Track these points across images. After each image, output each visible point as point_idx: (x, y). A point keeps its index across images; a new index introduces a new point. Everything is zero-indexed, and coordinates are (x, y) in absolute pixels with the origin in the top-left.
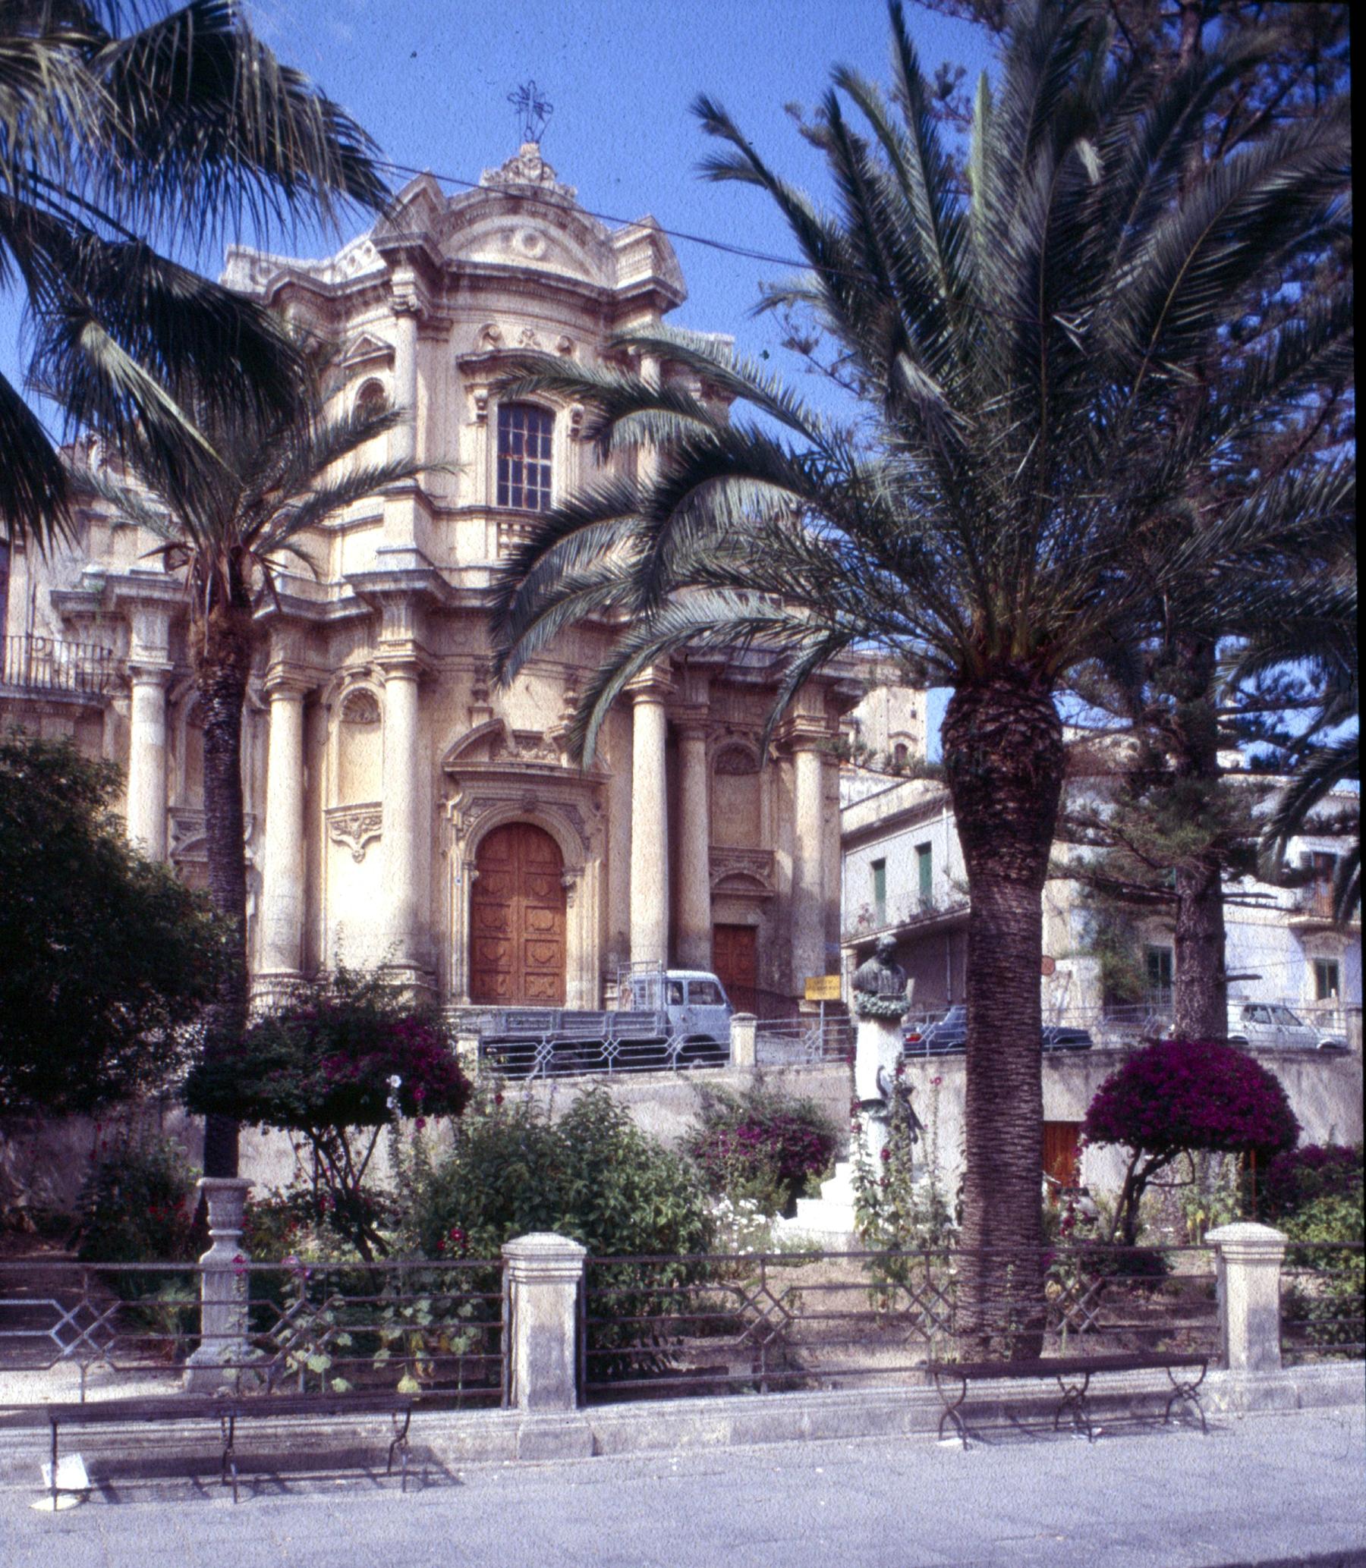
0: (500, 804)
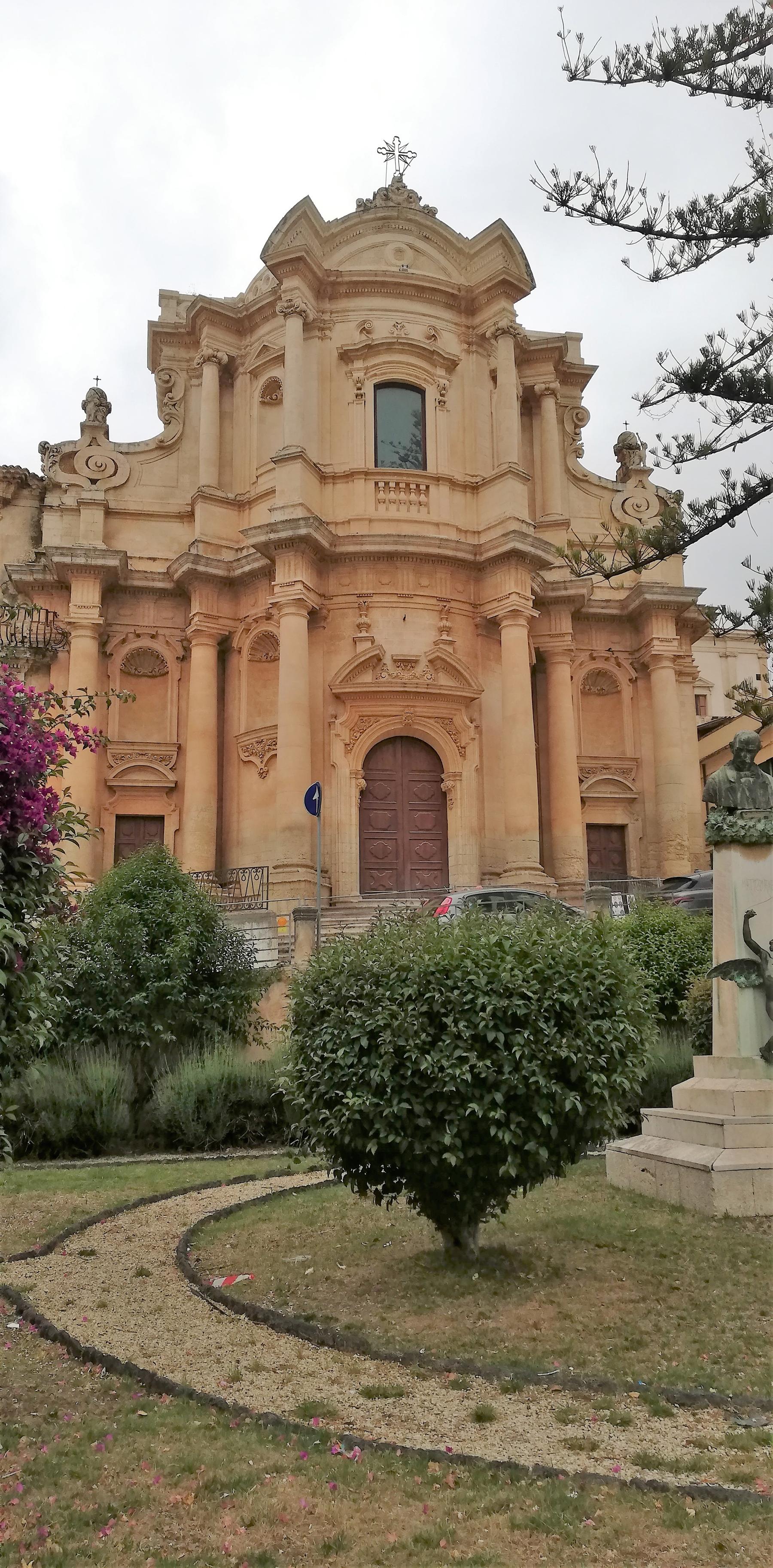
0: (383, 720)
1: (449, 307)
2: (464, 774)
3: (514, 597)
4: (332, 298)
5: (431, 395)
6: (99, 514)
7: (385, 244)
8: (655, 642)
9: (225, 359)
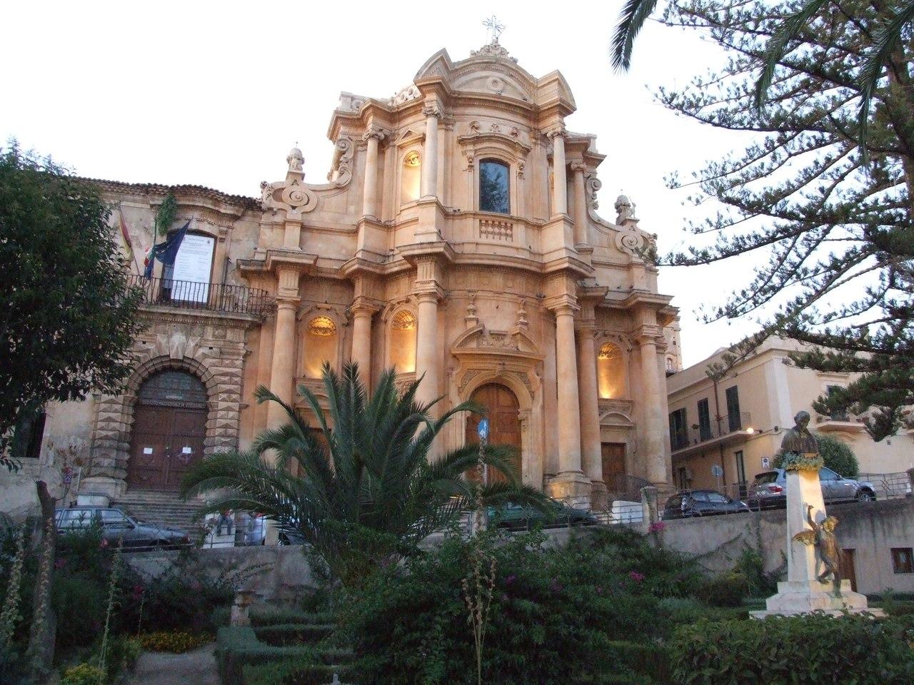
1: (524, 116)
2: (534, 410)
3: (565, 297)
4: (455, 106)
5: (514, 169)
6: (297, 230)
7: (487, 77)
8: (645, 328)
9: (383, 136)
